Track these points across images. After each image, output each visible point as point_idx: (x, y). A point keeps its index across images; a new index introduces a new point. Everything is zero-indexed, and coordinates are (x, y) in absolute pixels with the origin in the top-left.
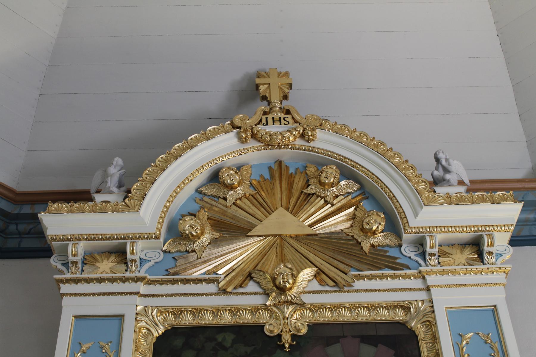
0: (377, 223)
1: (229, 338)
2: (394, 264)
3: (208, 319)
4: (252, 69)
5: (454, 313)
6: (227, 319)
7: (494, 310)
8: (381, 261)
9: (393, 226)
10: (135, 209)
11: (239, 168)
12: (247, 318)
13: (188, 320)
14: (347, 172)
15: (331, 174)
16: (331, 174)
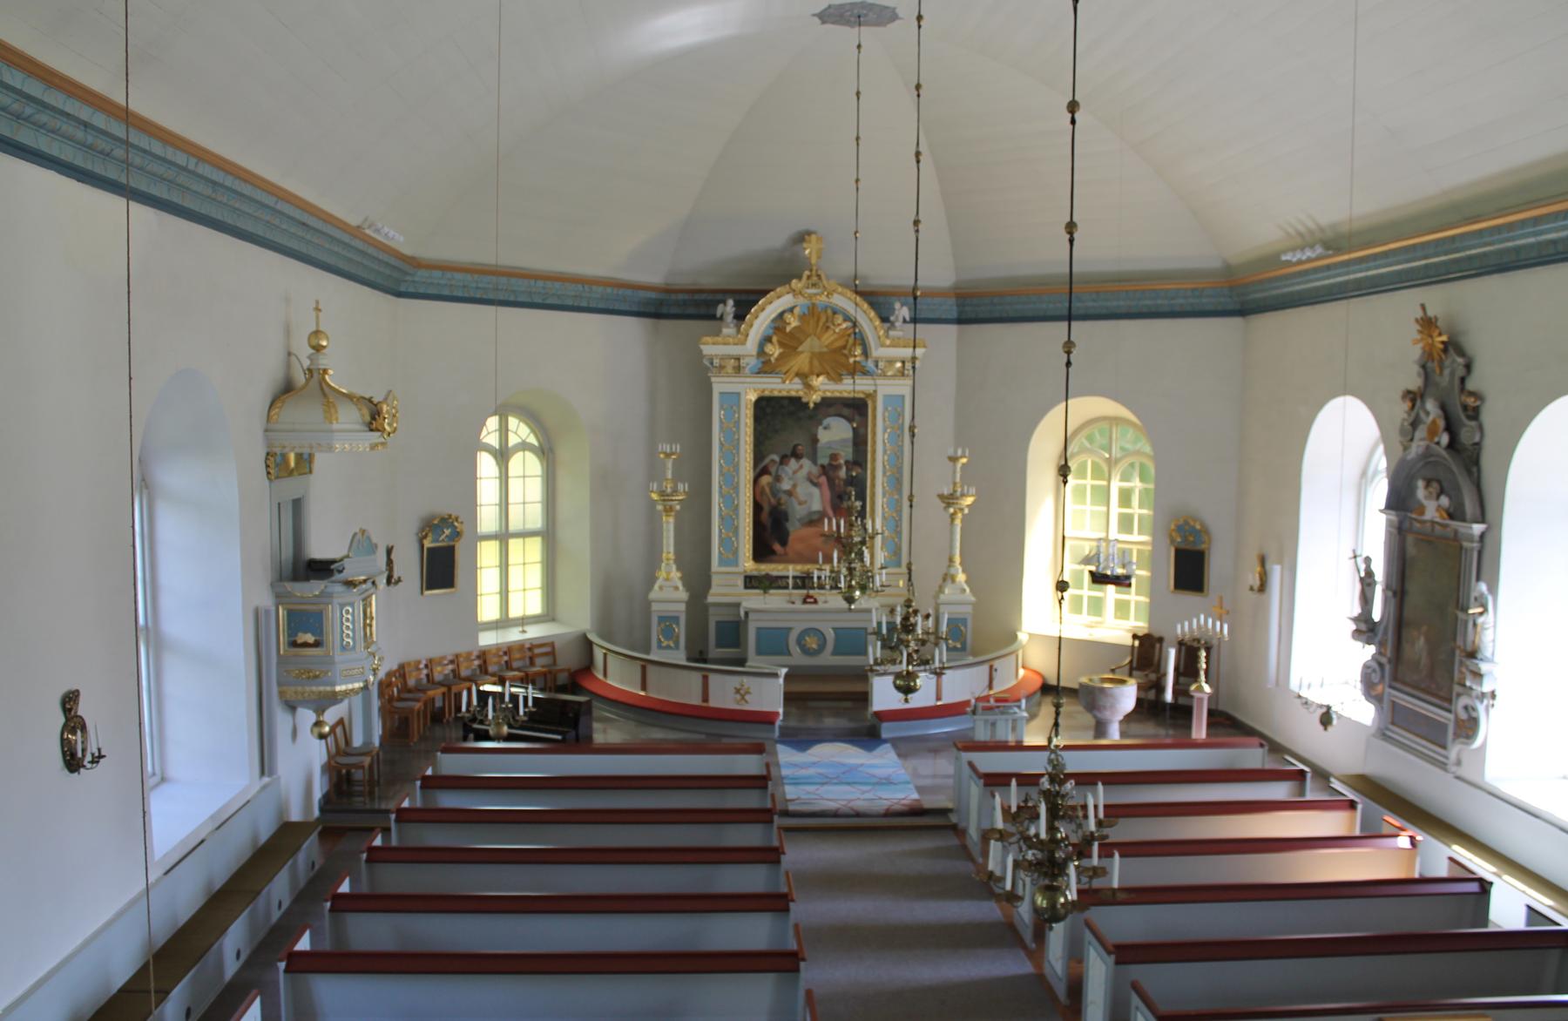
0: (858, 351)
1: (786, 403)
2: (866, 373)
3: (776, 394)
4: (803, 228)
5: (886, 397)
6: (784, 394)
7: (903, 397)
8: (856, 370)
9: (866, 353)
10: (743, 343)
11: (791, 310)
12: (793, 394)
13: (767, 393)
14: (847, 318)
15: (839, 319)
16: (839, 319)
